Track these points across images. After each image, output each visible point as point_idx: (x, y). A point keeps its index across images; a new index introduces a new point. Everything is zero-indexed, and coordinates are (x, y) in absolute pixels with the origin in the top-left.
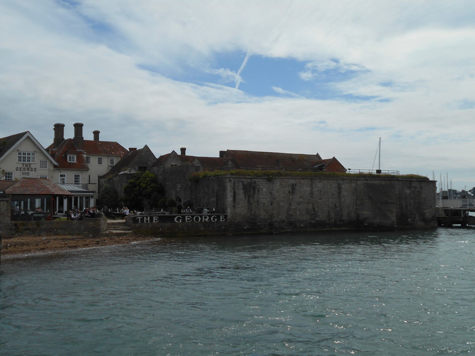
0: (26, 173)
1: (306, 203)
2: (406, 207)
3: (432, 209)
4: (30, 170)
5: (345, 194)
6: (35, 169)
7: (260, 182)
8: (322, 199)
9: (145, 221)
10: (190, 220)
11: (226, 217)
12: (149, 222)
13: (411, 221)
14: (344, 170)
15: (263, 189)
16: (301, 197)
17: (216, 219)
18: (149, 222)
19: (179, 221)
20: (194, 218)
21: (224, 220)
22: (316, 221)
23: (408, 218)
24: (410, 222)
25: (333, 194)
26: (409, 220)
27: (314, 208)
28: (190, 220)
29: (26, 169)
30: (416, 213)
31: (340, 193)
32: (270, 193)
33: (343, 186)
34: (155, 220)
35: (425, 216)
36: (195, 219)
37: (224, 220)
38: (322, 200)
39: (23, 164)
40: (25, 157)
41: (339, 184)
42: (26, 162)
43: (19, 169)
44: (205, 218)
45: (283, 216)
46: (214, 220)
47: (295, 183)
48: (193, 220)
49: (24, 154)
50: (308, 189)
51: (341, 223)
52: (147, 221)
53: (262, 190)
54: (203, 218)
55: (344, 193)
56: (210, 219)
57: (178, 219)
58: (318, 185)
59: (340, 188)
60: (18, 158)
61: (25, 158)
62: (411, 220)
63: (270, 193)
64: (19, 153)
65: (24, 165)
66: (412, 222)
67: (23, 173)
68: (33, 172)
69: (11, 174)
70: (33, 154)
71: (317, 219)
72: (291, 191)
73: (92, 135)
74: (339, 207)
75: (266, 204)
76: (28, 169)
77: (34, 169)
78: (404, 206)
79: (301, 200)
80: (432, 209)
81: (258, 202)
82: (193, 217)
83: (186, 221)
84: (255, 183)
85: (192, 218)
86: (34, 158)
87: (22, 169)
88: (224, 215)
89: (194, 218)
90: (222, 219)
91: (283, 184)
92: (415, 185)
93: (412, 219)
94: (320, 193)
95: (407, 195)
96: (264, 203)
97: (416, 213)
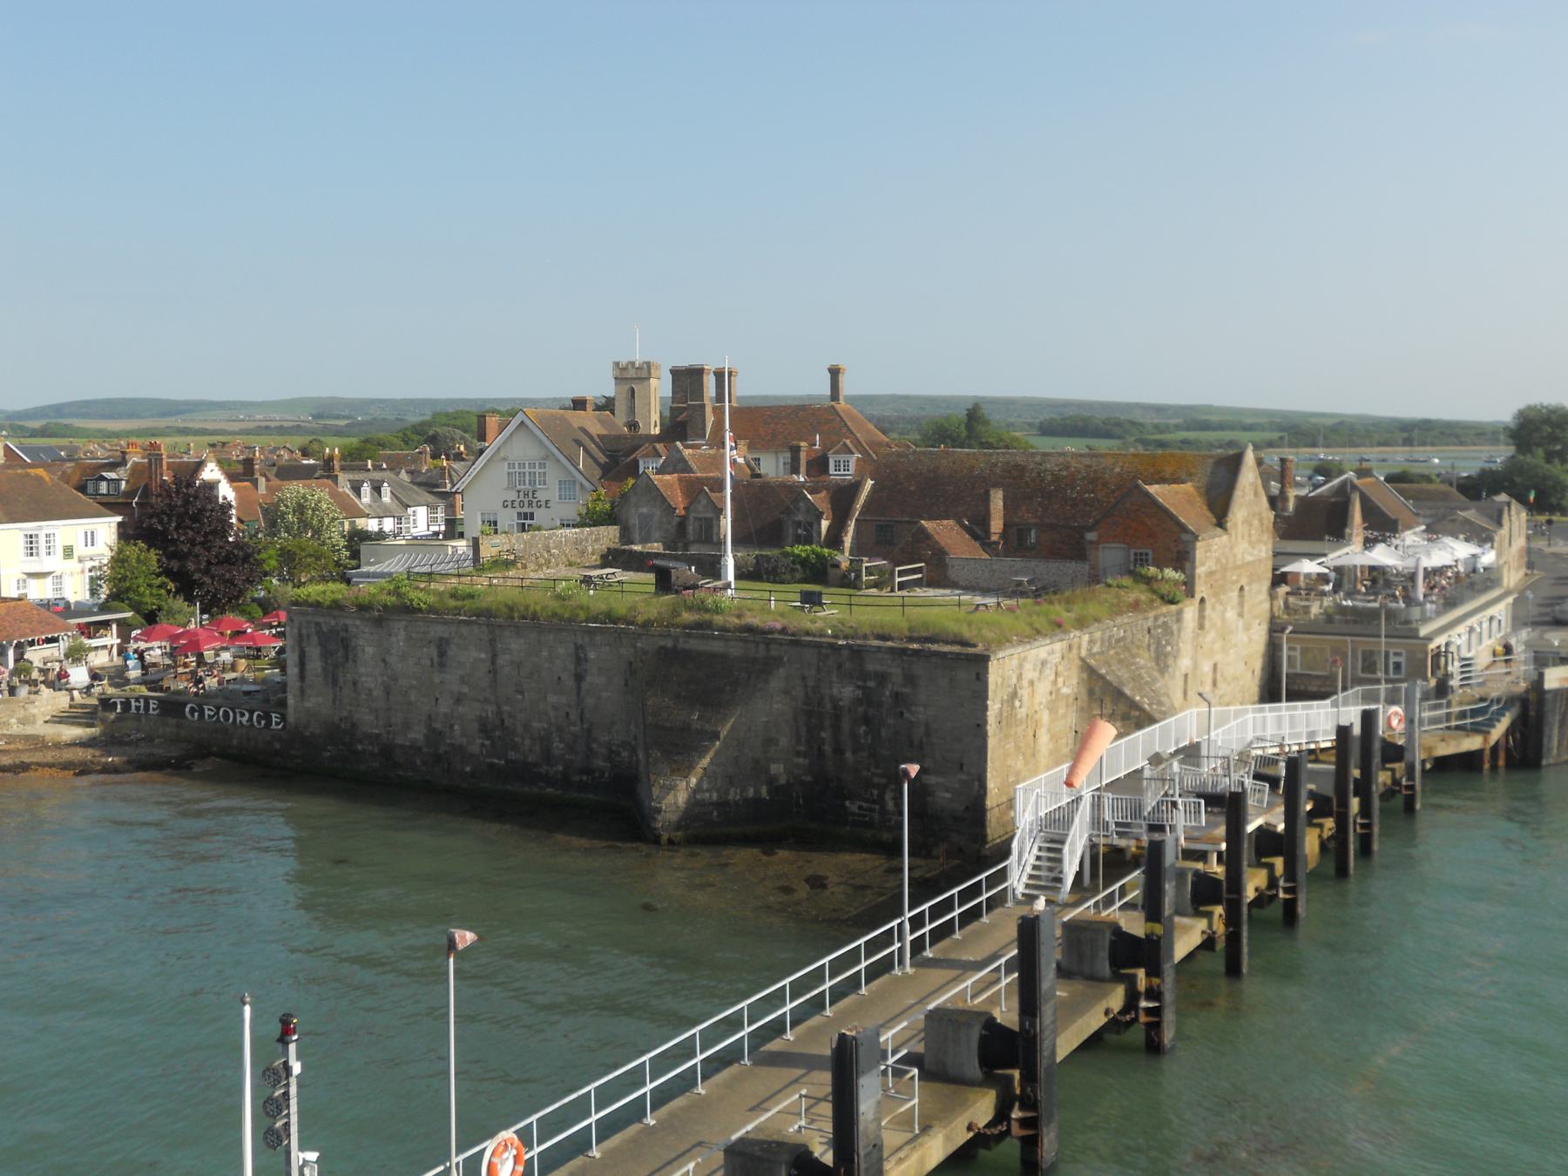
0: (525, 514)
1: (478, 701)
2: (839, 751)
3: (963, 777)
4: (534, 504)
6: (547, 502)
7: (357, 627)
8: (526, 694)
9: (133, 708)
10: (213, 716)
11: (283, 718)
12: (142, 711)
13: (857, 811)
14: (1185, 537)
15: (366, 649)
16: (463, 680)
17: (263, 722)
18: (142, 711)
19: (193, 716)
20: (221, 713)
21: (280, 727)
22: (509, 762)
23: (848, 798)
24: (853, 814)
25: (559, 678)
26: (852, 806)
27: (503, 721)
28: (213, 716)
29: (526, 504)
30: (883, 781)
31: (579, 678)
32: (384, 661)
33: (592, 655)
34: (154, 709)
35: (930, 799)
36: (223, 716)
37: (280, 727)
38: (523, 695)
39: (519, 492)
41: (578, 648)
42: (527, 486)
43: (510, 504)
44: (242, 715)
45: (417, 734)
46: (259, 723)
47: (446, 635)
48: (218, 718)
49: (522, 465)
50: (483, 656)
51: (585, 778)
52: (138, 708)
53: (364, 650)
54: (238, 716)
55: (593, 679)
56: (251, 719)
57: (192, 711)
58: (513, 646)
59: (579, 659)
60: (506, 477)
61: (524, 477)
62: (860, 808)
63: (384, 661)
64: (509, 464)
65: (522, 494)
66: (859, 815)
67: (519, 514)
68: (543, 509)
70: (542, 465)
71: (512, 755)
72: (436, 659)
73: (827, 378)
74: (578, 722)
75: (375, 693)
76: (530, 504)
77: (543, 504)
78: (827, 748)
79: (466, 689)
80: (963, 777)
81: (355, 684)
82: (218, 708)
83: (206, 717)
84: (347, 631)
85: (218, 713)
86: (545, 473)
87: (516, 504)
88: (281, 714)
89: (221, 713)
90: (277, 724)
91: (414, 635)
92: (878, 668)
93: (865, 805)
94: (519, 673)
95: (841, 703)
96: (370, 690)
97: (883, 781)
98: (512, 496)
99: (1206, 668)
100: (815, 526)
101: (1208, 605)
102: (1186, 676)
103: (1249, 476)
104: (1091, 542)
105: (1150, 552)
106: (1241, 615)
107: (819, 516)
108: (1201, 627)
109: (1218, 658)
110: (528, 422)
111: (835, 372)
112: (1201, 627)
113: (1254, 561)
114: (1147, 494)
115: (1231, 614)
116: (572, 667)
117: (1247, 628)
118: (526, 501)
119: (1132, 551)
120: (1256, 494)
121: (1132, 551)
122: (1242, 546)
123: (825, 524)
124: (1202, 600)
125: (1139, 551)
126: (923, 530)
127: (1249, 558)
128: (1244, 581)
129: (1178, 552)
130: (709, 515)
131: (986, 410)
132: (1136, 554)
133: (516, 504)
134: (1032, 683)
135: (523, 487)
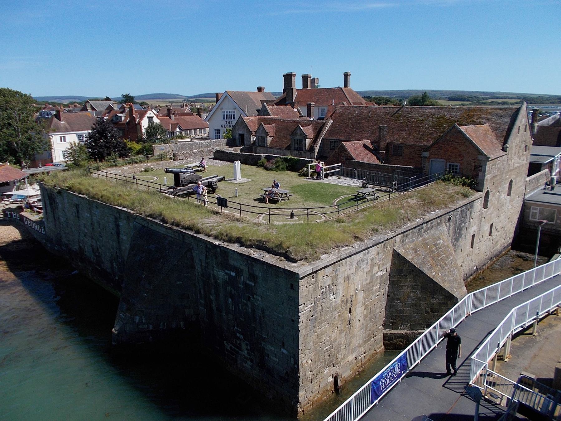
5: (125, 238)
14: (480, 157)
24: (227, 350)
29: (229, 126)
39: (226, 122)
40: (228, 115)
41: (116, 218)
43: (224, 126)
65: (227, 122)
69: (219, 130)
78: (214, 306)
87: (226, 126)
98: (224, 123)
99: (487, 228)
100: (304, 141)
101: (491, 195)
102: (473, 236)
103: (522, 120)
104: (425, 158)
105: (459, 164)
106: (509, 195)
107: (306, 137)
108: (485, 206)
109: (494, 220)
110: (228, 96)
111: (346, 75)
112: (485, 206)
113: (519, 167)
114: (460, 132)
115: (504, 196)
116: (115, 228)
117: (511, 201)
118: (229, 125)
119: (448, 164)
120: (525, 131)
121: (448, 164)
122: (515, 159)
123: (308, 141)
124: (488, 193)
125: (452, 164)
126: (343, 146)
127: (516, 165)
128: (513, 177)
129: (475, 166)
130: (264, 135)
131: (427, 92)
132: (450, 165)
133: (226, 126)
134: (348, 278)
135: (227, 120)
